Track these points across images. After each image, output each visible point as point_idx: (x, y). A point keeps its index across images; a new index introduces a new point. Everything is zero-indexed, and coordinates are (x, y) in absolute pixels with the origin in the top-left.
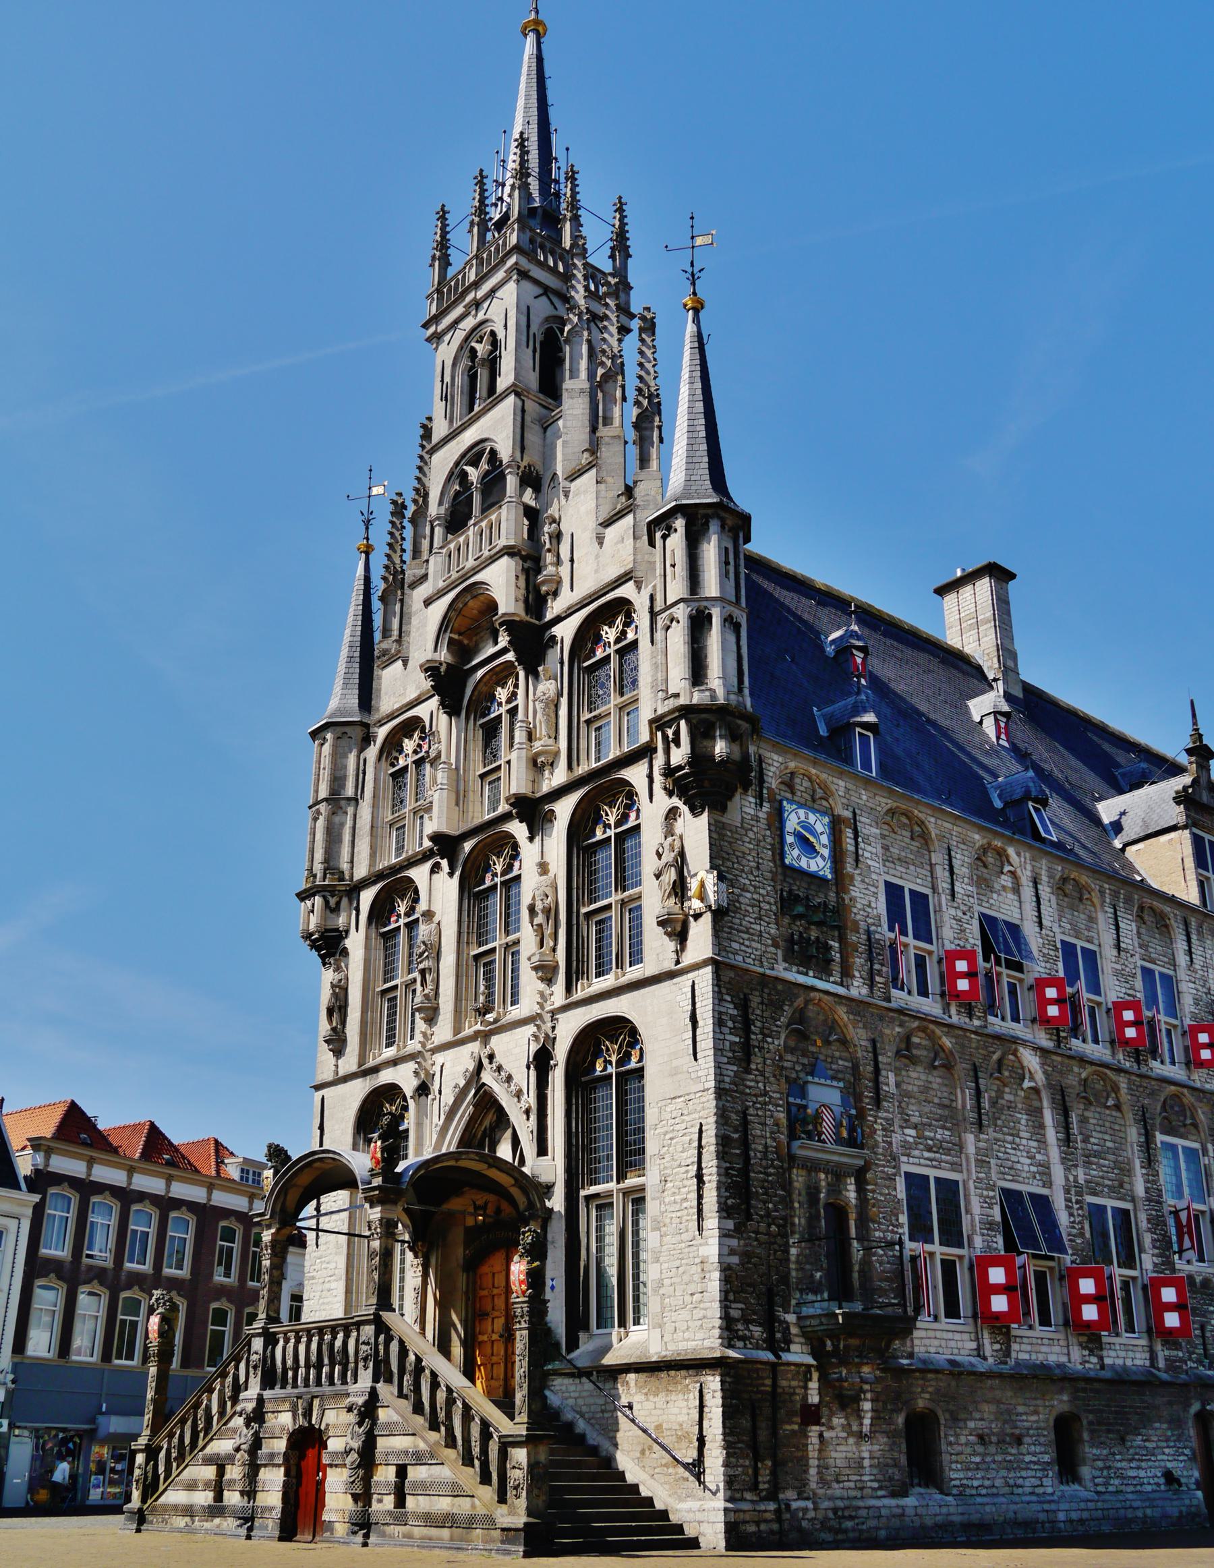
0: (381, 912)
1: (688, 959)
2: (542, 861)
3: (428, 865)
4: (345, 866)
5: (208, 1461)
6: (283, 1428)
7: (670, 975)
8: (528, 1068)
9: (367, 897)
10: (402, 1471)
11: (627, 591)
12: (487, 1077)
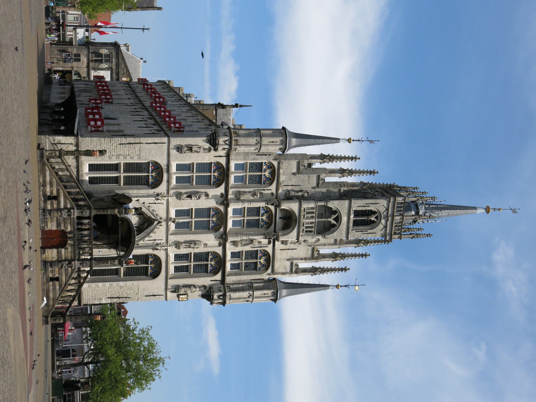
0: (218, 164)
1: (169, 293)
2: (209, 242)
3: (223, 191)
4: (237, 151)
5: (58, 191)
6: (67, 228)
7: (166, 289)
8: (155, 240)
9: (223, 161)
10: (57, 279)
11: (269, 271)
12: (156, 222)
